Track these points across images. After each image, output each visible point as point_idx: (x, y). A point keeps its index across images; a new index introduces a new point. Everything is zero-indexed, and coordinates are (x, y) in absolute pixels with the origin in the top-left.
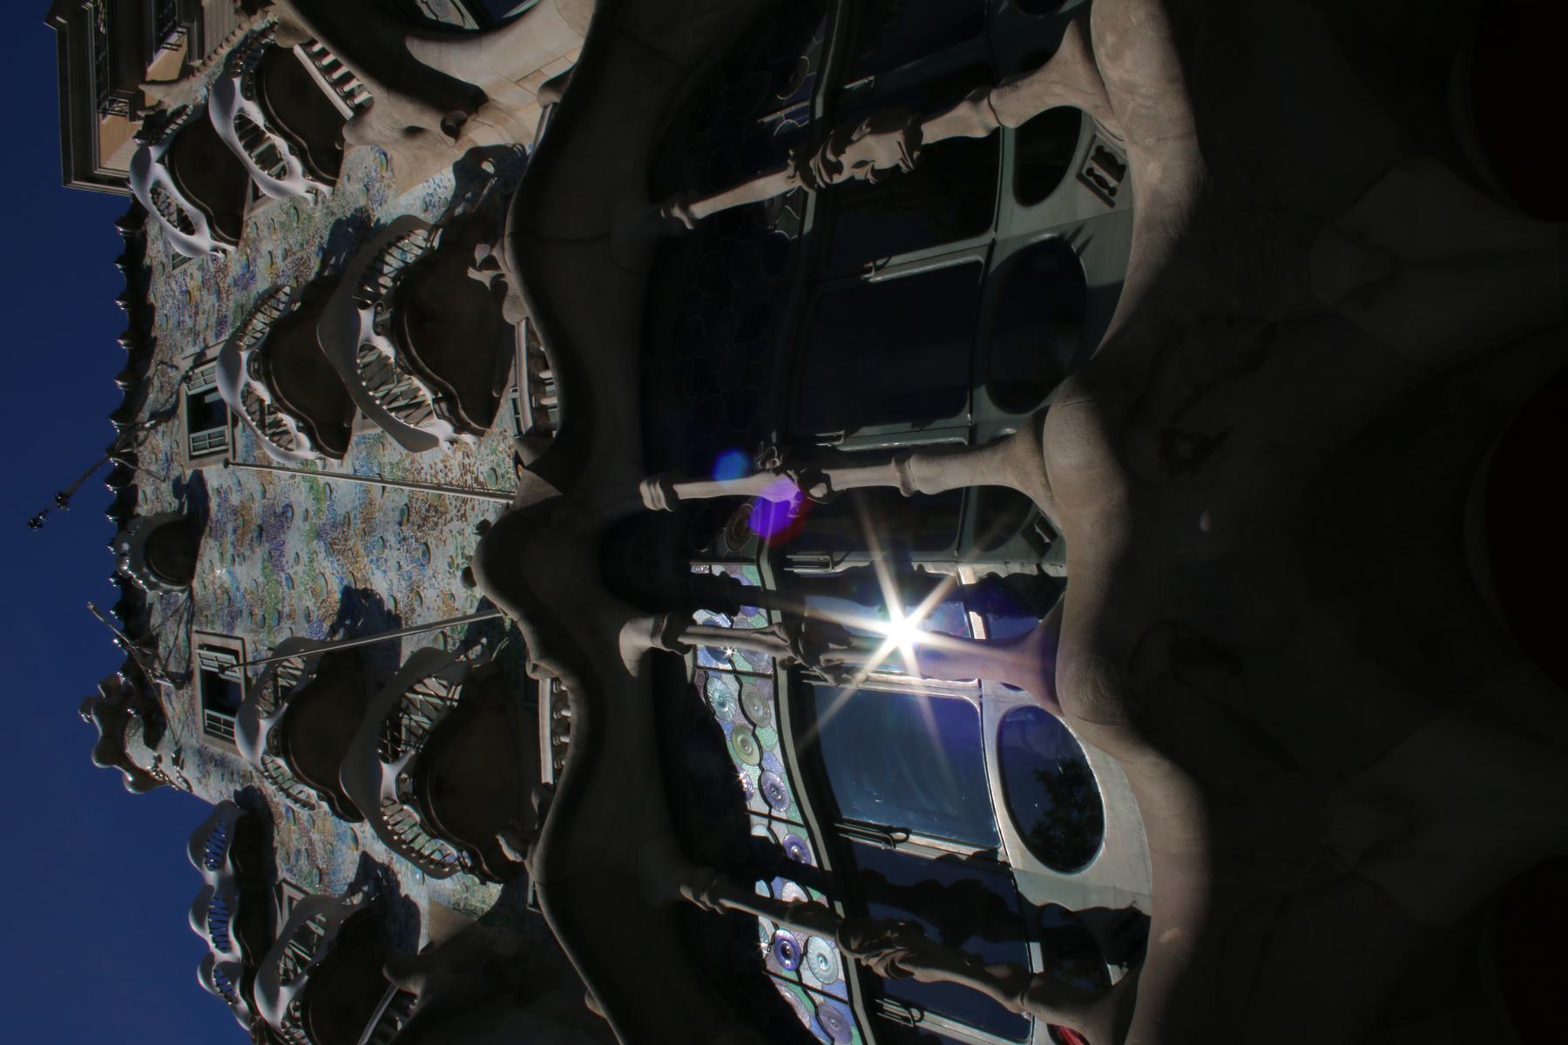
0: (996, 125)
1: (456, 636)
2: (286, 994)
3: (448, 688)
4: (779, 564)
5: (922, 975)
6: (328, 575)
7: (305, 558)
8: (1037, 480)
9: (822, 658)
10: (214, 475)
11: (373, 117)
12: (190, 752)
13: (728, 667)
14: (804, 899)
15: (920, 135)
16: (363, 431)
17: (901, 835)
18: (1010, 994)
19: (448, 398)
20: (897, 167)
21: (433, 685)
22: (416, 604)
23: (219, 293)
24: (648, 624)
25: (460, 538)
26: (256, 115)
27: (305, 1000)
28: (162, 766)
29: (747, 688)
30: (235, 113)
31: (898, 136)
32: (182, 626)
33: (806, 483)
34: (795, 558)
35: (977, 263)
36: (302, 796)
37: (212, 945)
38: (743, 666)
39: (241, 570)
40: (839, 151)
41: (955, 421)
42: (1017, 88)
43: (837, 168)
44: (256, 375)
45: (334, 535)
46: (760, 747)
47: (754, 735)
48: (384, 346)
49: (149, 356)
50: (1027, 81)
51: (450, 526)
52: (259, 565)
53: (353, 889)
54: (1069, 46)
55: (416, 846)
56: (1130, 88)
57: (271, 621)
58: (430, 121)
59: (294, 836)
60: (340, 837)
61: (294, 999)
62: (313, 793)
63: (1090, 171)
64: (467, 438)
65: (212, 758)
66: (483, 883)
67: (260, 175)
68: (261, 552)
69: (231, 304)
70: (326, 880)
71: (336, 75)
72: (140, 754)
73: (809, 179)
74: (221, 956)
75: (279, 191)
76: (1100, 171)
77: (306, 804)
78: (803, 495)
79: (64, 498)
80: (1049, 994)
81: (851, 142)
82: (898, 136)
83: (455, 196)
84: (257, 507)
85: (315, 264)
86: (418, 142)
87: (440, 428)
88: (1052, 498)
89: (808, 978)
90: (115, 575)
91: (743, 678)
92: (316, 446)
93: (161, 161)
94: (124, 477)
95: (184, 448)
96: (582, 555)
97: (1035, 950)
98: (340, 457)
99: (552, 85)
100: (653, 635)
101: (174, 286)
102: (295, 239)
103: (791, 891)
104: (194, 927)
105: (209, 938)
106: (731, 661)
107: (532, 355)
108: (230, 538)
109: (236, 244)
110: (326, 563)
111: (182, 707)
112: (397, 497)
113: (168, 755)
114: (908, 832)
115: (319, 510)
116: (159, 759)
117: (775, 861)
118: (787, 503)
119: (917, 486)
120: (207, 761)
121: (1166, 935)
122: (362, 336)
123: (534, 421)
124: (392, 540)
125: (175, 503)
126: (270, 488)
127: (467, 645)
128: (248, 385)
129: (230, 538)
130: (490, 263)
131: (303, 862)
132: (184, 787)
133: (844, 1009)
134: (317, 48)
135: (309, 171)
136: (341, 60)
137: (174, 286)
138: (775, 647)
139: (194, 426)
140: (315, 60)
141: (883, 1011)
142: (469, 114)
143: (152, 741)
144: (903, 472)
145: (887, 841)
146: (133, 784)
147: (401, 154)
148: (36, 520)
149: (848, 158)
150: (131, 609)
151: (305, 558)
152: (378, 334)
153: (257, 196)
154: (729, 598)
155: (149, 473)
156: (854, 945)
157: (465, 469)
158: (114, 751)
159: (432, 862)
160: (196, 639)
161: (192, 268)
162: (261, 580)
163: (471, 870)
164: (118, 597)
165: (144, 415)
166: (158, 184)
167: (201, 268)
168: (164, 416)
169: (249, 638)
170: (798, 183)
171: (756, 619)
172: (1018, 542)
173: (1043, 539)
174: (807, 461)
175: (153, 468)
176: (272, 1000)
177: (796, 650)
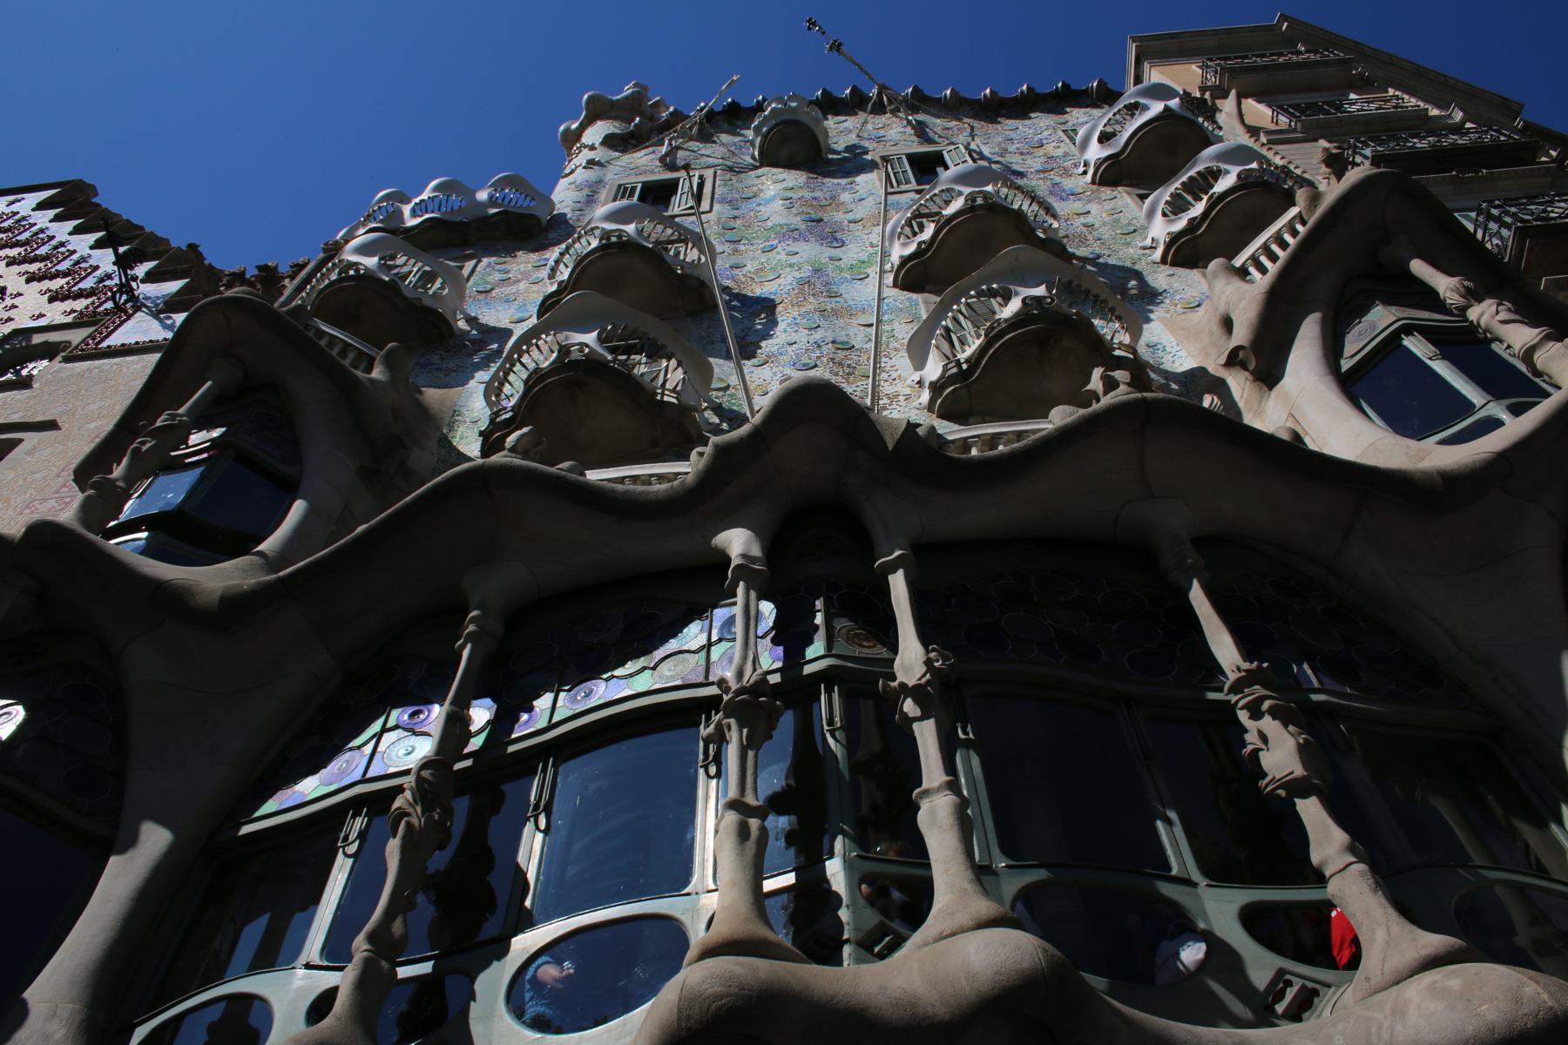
0: (1327, 873)
2: (371, 262)
3: (674, 390)
5: (393, 848)
7: (793, 260)
9: (732, 721)
10: (870, 182)
11: (1237, 284)
13: (714, 638)
14: (473, 728)
15: (1305, 796)
16: (923, 304)
17: (542, 825)
18: (371, 938)
19: (962, 376)
20: (1265, 775)
21: (676, 376)
23: (1044, 171)
24: (756, 551)
26: (1221, 186)
27: (366, 279)
28: (585, 151)
29: (693, 658)
30: (1223, 166)
31: (1299, 771)
32: (716, 161)
33: (917, 693)
34: (836, 696)
35: (1169, 869)
36: (562, 266)
37: (417, 200)
38: (716, 652)
39: (778, 205)
40: (1274, 713)
41: (996, 850)
42: (1375, 891)
43: (1256, 714)
44: (971, 198)
45: (818, 283)
46: (631, 675)
47: (644, 668)
49: (975, 117)
50: (1384, 902)
52: (783, 221)
53: (472, 321)
54: (1434, 942)
55: (518, 367)
56: (1399, 1012)
57: (730, 235)
58: (1242, 334)
59: (522, 267)
61: (366, 269)
62: (566, 277)
63: (1289, 984)
64: (925, 396)
66: (481, 434)
67: (1164, 194)
68: (796, 221)
69: (1034, 182)
71: (1274, 247)
72: (596, 133)
74: (407, 210)
75: (1151, 214)
76: (1290, 994)
77: (554, 270)
78: (904, 690)
79: (836, 47)
80: (373, 983)
81: (1286, 726)
82: (1299, 771)
84: (839, 216)
85: (1082, 252)
86: (1217, 330)
87: (934, 369)
88: (926, 944)
89: (388, 738)
90: (764, 100)
91: (703, 653)
92: (905, 261)
93: (1167, 109)
94: (856, 104)
95: (890, 151)
96: (823, 484)
97: (426, 968)
98: (895, 285)
99: (1297, 437)
100: (744, 556)
101: (1046, 133)
102: (1106, 233)
103: (481, 714)
104: (433, 184)
105: (424, 196)
106: (720, 640)
107: (1020, 435)
108: (808, 195)
109: (1093, 182)
110: (790, 279)
111: (644, 164)
112: (860, 338)
113: (596, 155)
114: (546, 832)
115: (842, 270)
116: (592, 148)
118: (894, 678)
119: (925, 808)
122: (1019, 289)
123: (953, 441)
124: (818, 335)
125: (840, 147)
126: (859, 226)
127: (717, 409)
128: (960, 194)
129: (808, 195)
130: (1110, 384)
131: (498, 276)
133: (357, 775)
134: (1299, 227)
135: (1174, 239)
136: (1289, 250)
137: (1046, 133)
138: (740, 674)
139: (913, 159)
140: (1284, 231)
141: (354, 817)
142: (1252, 373)
143: (609, 141)
144: (939, 789)
145: (536, 807)
146: (567, 130)
147: (1205, 319)
148: (814, 24)
149: (1269, 724)
150: (733, 116)
151: (793, 260)
152: (1024, 301)
153: (1143, 197)
154: (791, 635)
155: (866, 122)
156: (426, 774)
158: (598, 109)
159: (501, 384)
160: (711, 171)
161: (1066, 146)
162: (769, 224)
163: (492, 421)
164: (745, 103)
165: (921, 117)
166: (1146, 108)
167: (1066, 155)
168: (921, 131)
169: (712, 217)
170: (1232, 676)
171: (770, 659)
172: (872, 918)
173: (880, 943)
174: (940, 695)
175: (870, 126)
176: (364, 250)
177: (738, 692)
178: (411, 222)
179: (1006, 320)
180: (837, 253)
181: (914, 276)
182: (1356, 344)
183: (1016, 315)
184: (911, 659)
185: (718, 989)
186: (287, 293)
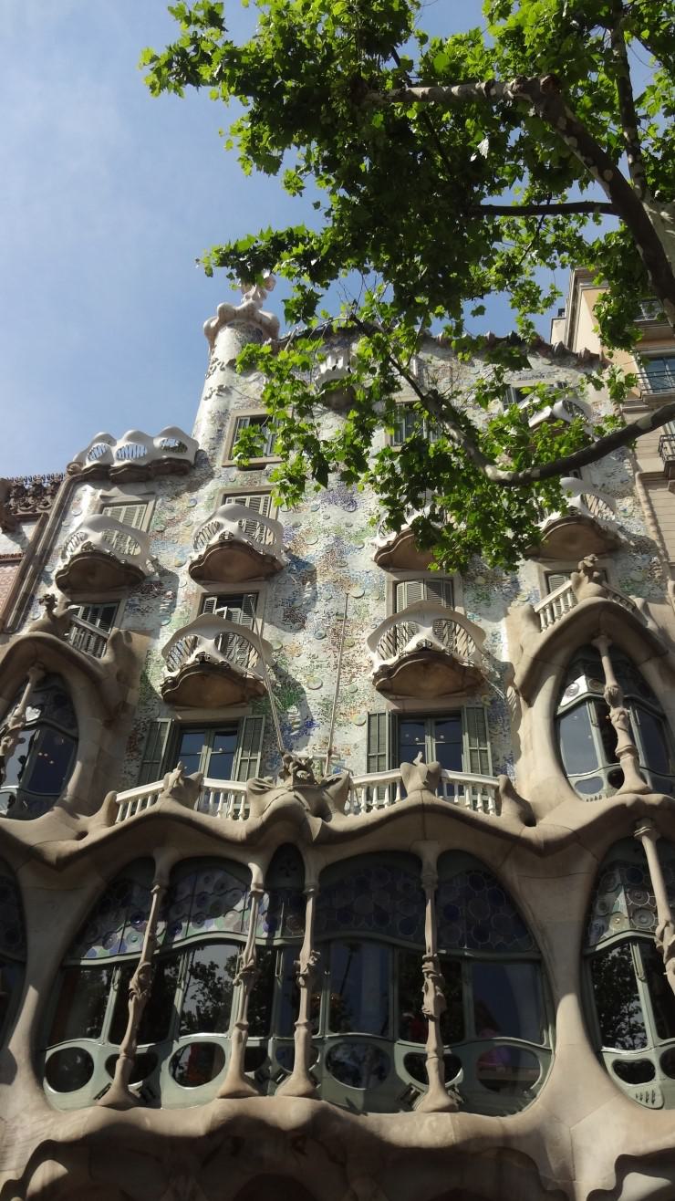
1: (280, 658)
4: (280, 948)
6: (317, 545)
7: (328, 525)
8: (289, 1092)
12: (225, 401)
15: (432, 1020)
22: (297, 624)
24: (261, 881)
25: (326, 663)
33: (305, 977)
40: (432, 978)
48: (411, 646)
51: (333, 655)
53: (155, 562)
60: (182, 554)
65: (222, 425)
70: (159, 536)
73: (428, 960)
74: (115, 450)
78: (300, 975)
83: (495, 660)
87: (378, 660)
117: (172, 930)
120: (221, 417)
121: (149, 1118)
132: (206, 393)
146: (208, 327)
156: (141, 976)
157: (358, 667)
158: (227, 318)
178: (117, 464)
179: (408, 653)
180: (349, 517)
181: (387, 559)
182: (566, 701)
183: (414, 651)
184: (306, 958)
185: (222, 1118)
186: (52, 513)
